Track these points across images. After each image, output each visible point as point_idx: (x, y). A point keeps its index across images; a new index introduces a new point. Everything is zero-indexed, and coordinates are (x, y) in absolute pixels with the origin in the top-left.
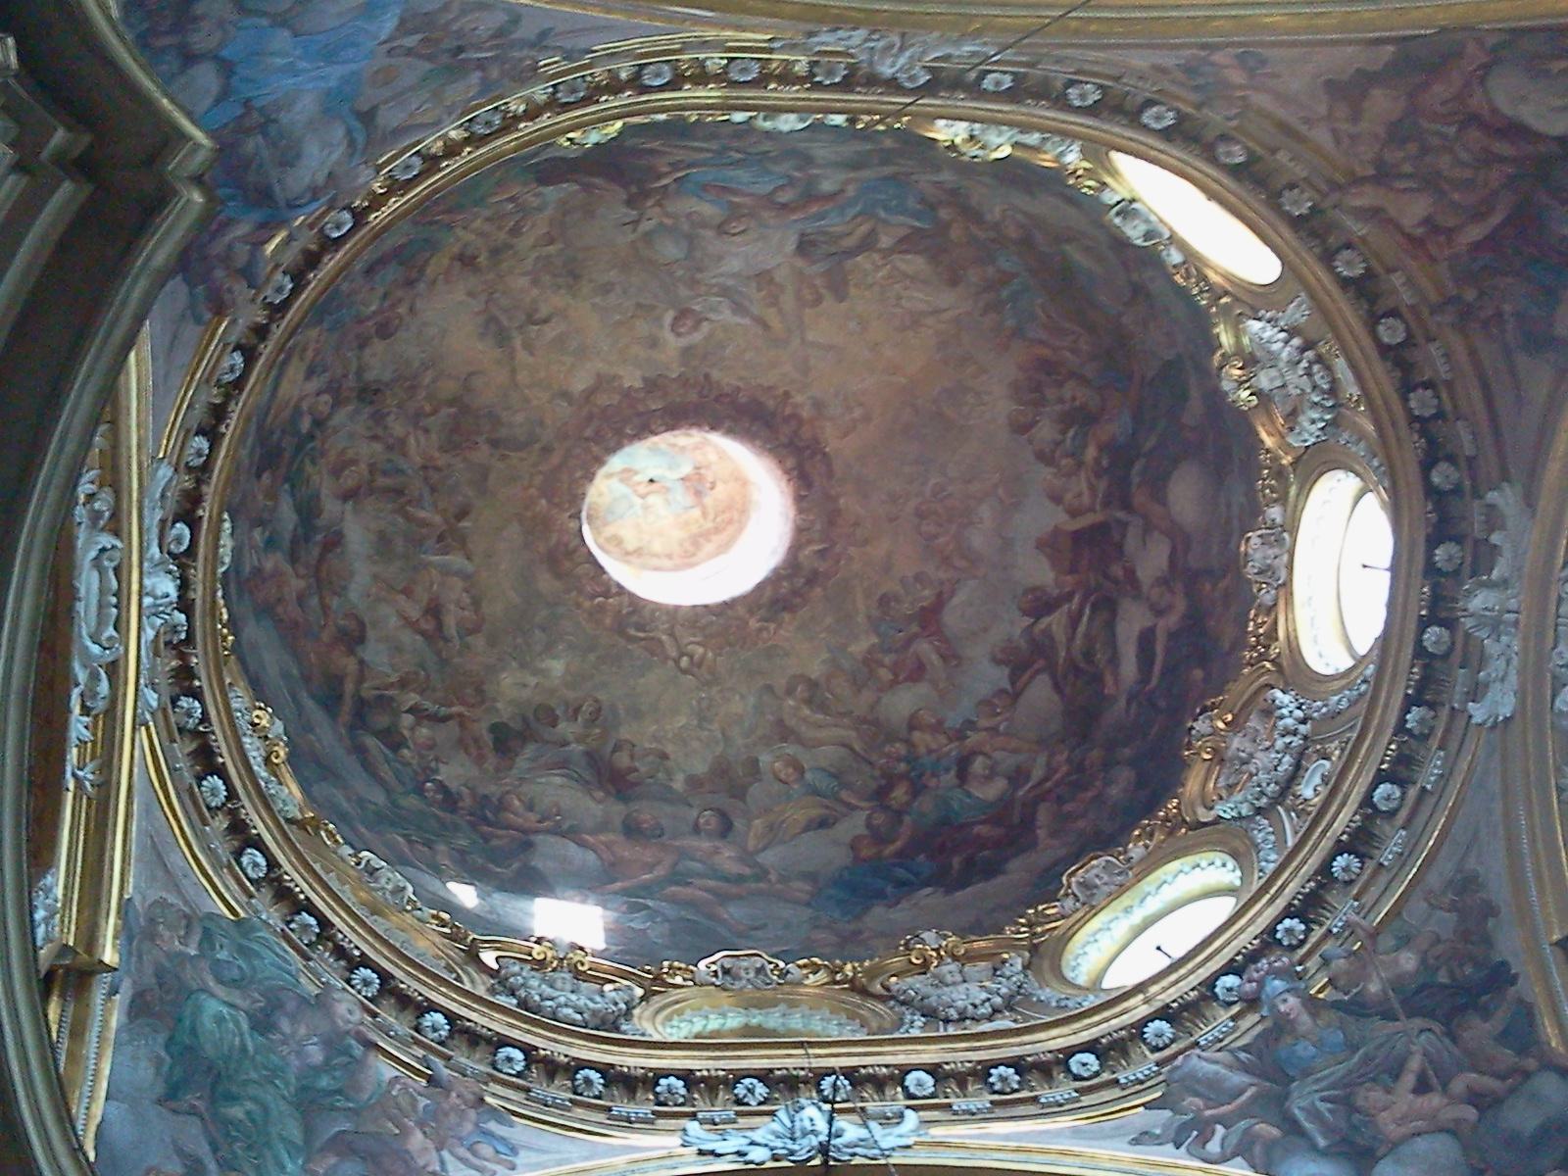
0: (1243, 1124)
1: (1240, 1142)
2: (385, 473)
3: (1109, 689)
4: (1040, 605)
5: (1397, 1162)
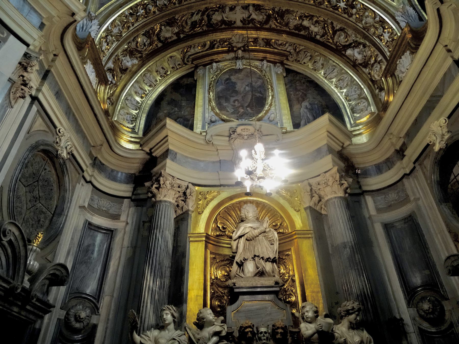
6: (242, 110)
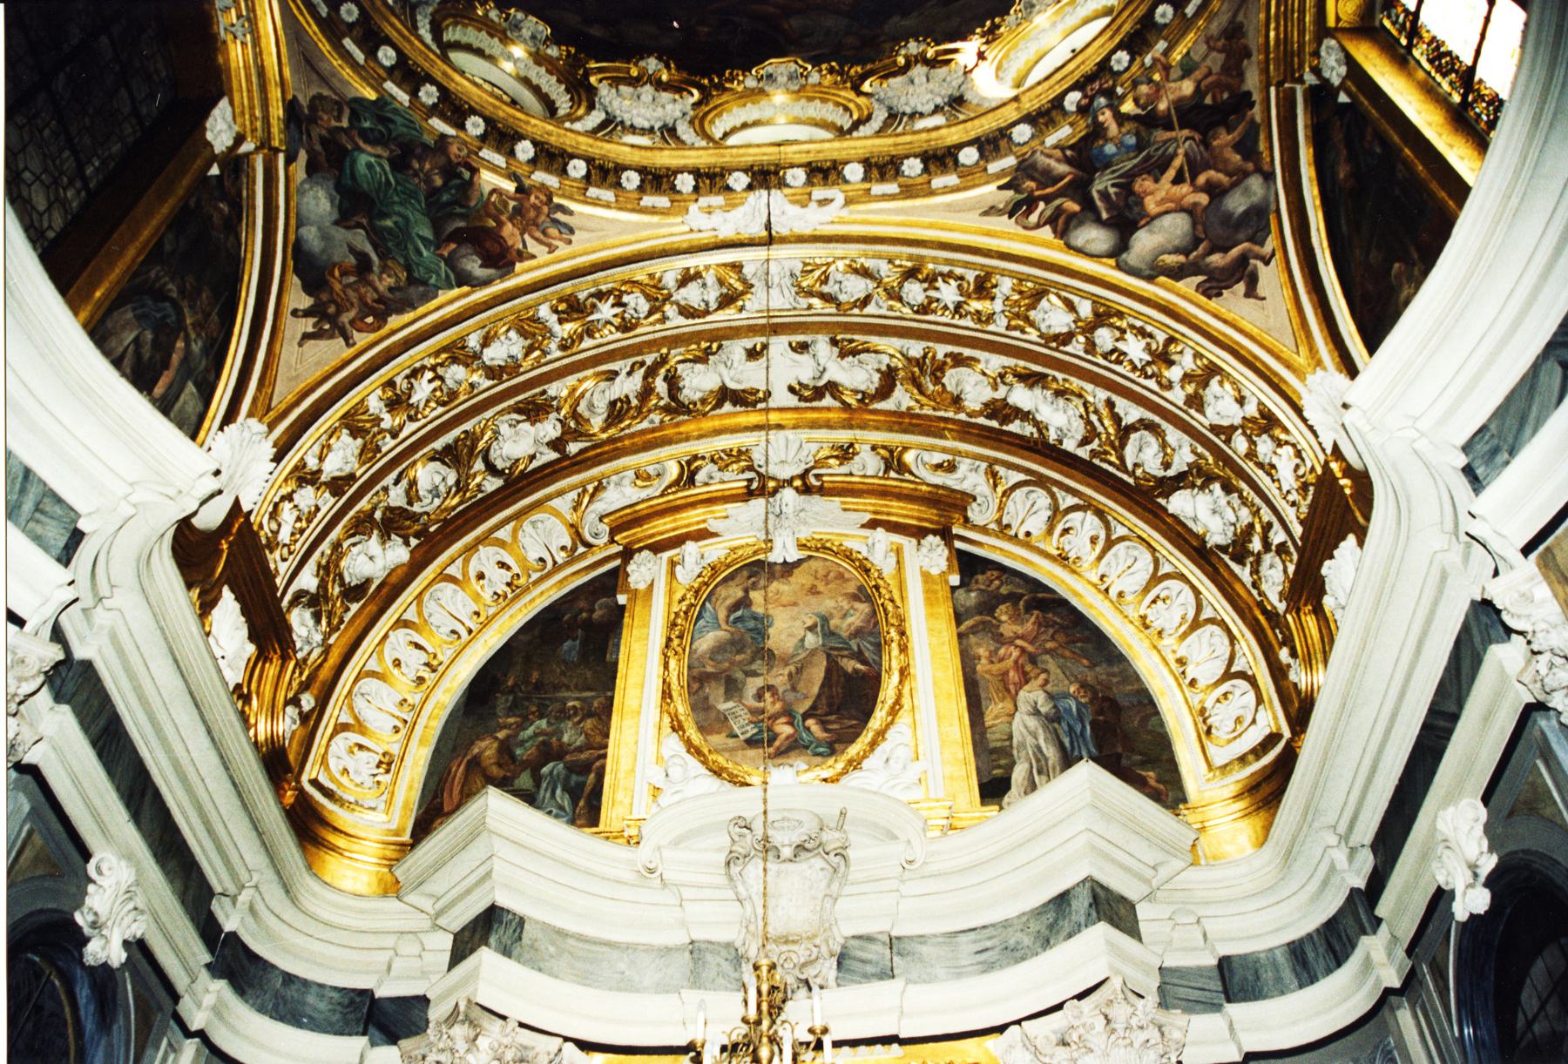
0: (1058, 202)
1: (1050, 217)
5: (1150, 231)
6: (788, 730)
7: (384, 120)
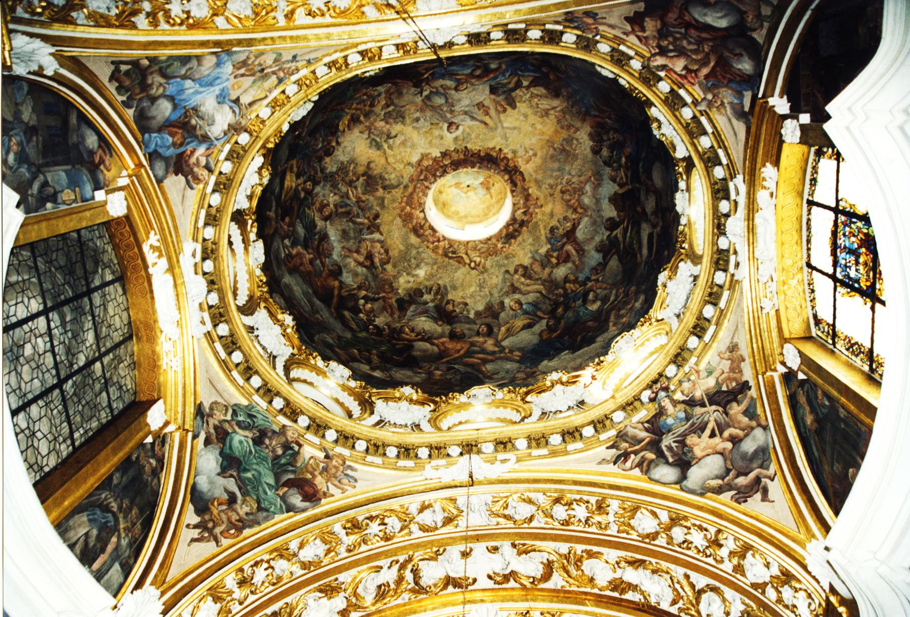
0: (642, 454)
2: (341, 207)
3: (639, 260)
4: (612, 225)
5: (700, 467)
7: (251, 416)
